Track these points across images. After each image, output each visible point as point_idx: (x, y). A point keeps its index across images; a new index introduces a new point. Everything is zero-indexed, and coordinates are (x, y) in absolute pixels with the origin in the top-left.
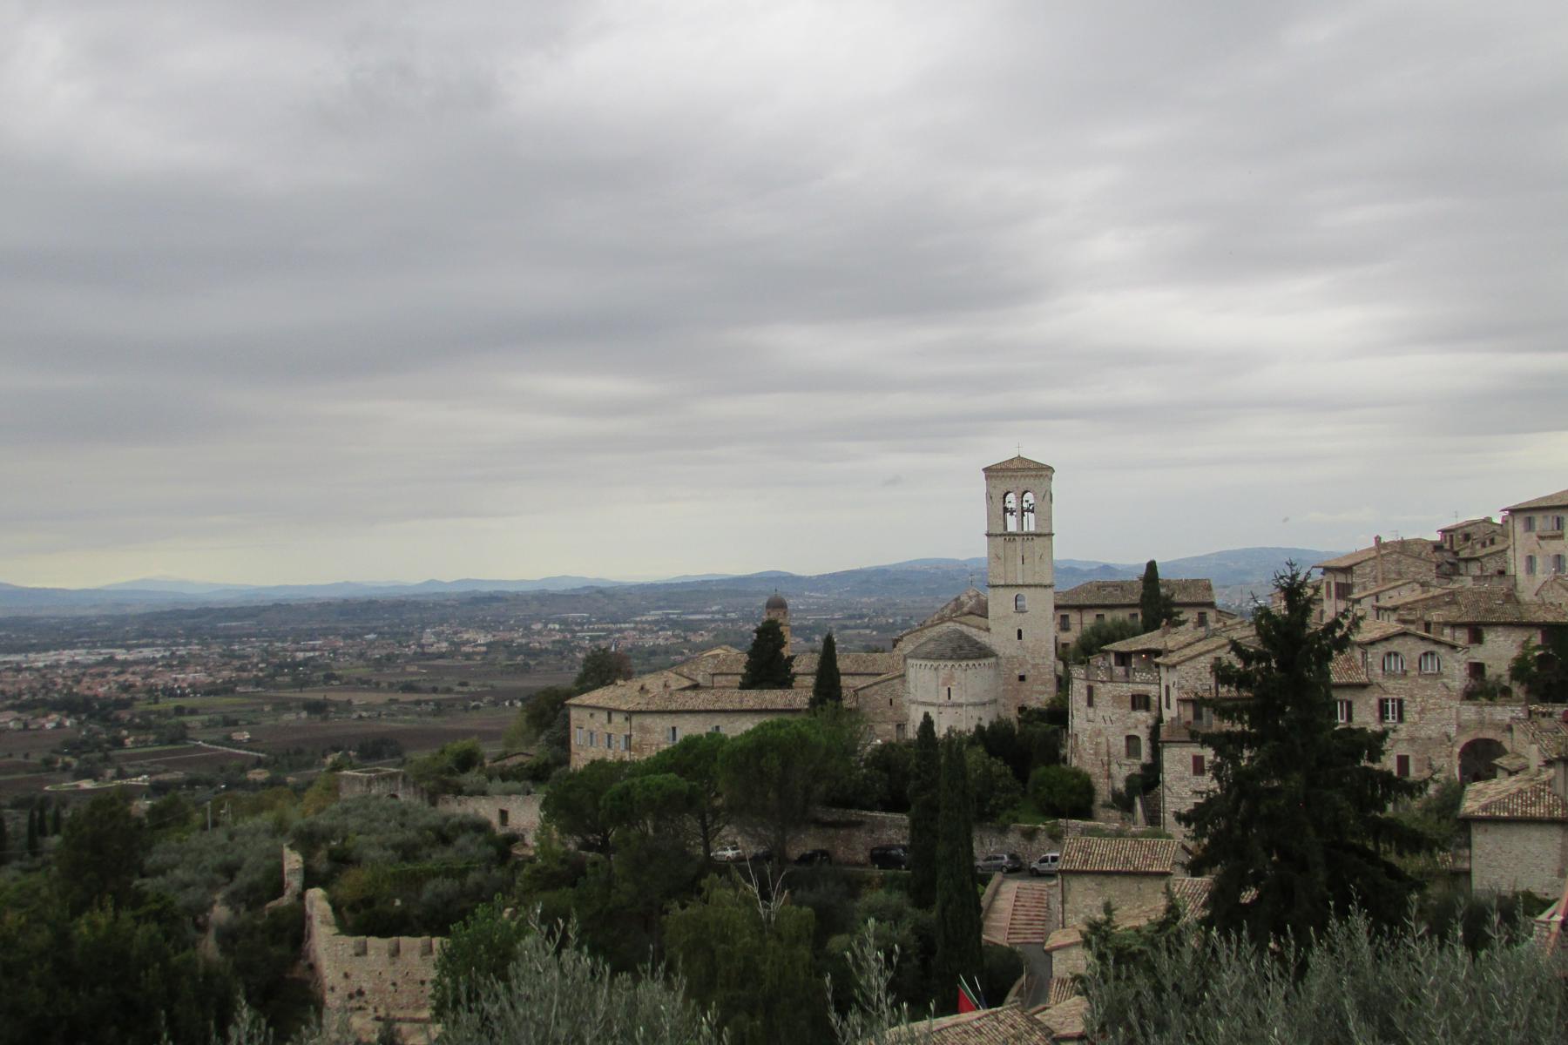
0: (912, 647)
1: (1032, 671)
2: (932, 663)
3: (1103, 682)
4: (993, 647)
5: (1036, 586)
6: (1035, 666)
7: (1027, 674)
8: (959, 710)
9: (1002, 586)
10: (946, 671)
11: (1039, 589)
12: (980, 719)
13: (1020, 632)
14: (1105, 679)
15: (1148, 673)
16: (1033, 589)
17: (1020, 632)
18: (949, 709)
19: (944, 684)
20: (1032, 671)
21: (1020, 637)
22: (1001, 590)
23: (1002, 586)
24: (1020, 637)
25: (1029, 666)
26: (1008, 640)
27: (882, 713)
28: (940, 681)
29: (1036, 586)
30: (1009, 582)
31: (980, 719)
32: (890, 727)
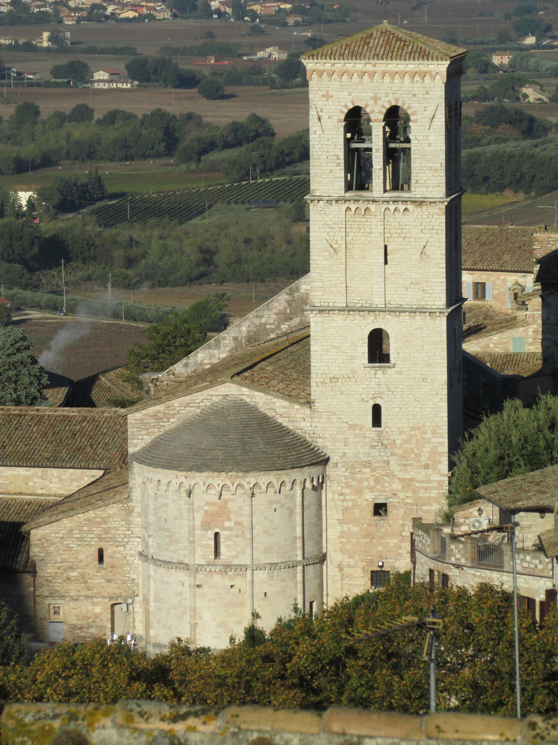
0: (148, 439)
1: (401, 495)
2: (184, 480)
3: (458, 566)
4: (319, 443)
5: (413, 311)
6: (407, 484)
7: (391, 502)
8: (238, 582)
9: (341, 310)
10: (212, 496)
11: (418, 317)
12: (256, 616)
13: (377, 410)
14: (463, 561)
15: (534, 558)
16: (405, 317)
17: (377, 410)
18: (217, 578)
19: (206, 526)
20: (401, 495)
21: (377, 420)
22: (338, 319)
23: (341, 310)
24: (377, 420)
25: (396, 486)
26: (352, 427)
27: (83, 579)
28: (199, 518)
29: (413, 311)
30: (355, 300)
31: (256, 616)
32: (98, 610)
